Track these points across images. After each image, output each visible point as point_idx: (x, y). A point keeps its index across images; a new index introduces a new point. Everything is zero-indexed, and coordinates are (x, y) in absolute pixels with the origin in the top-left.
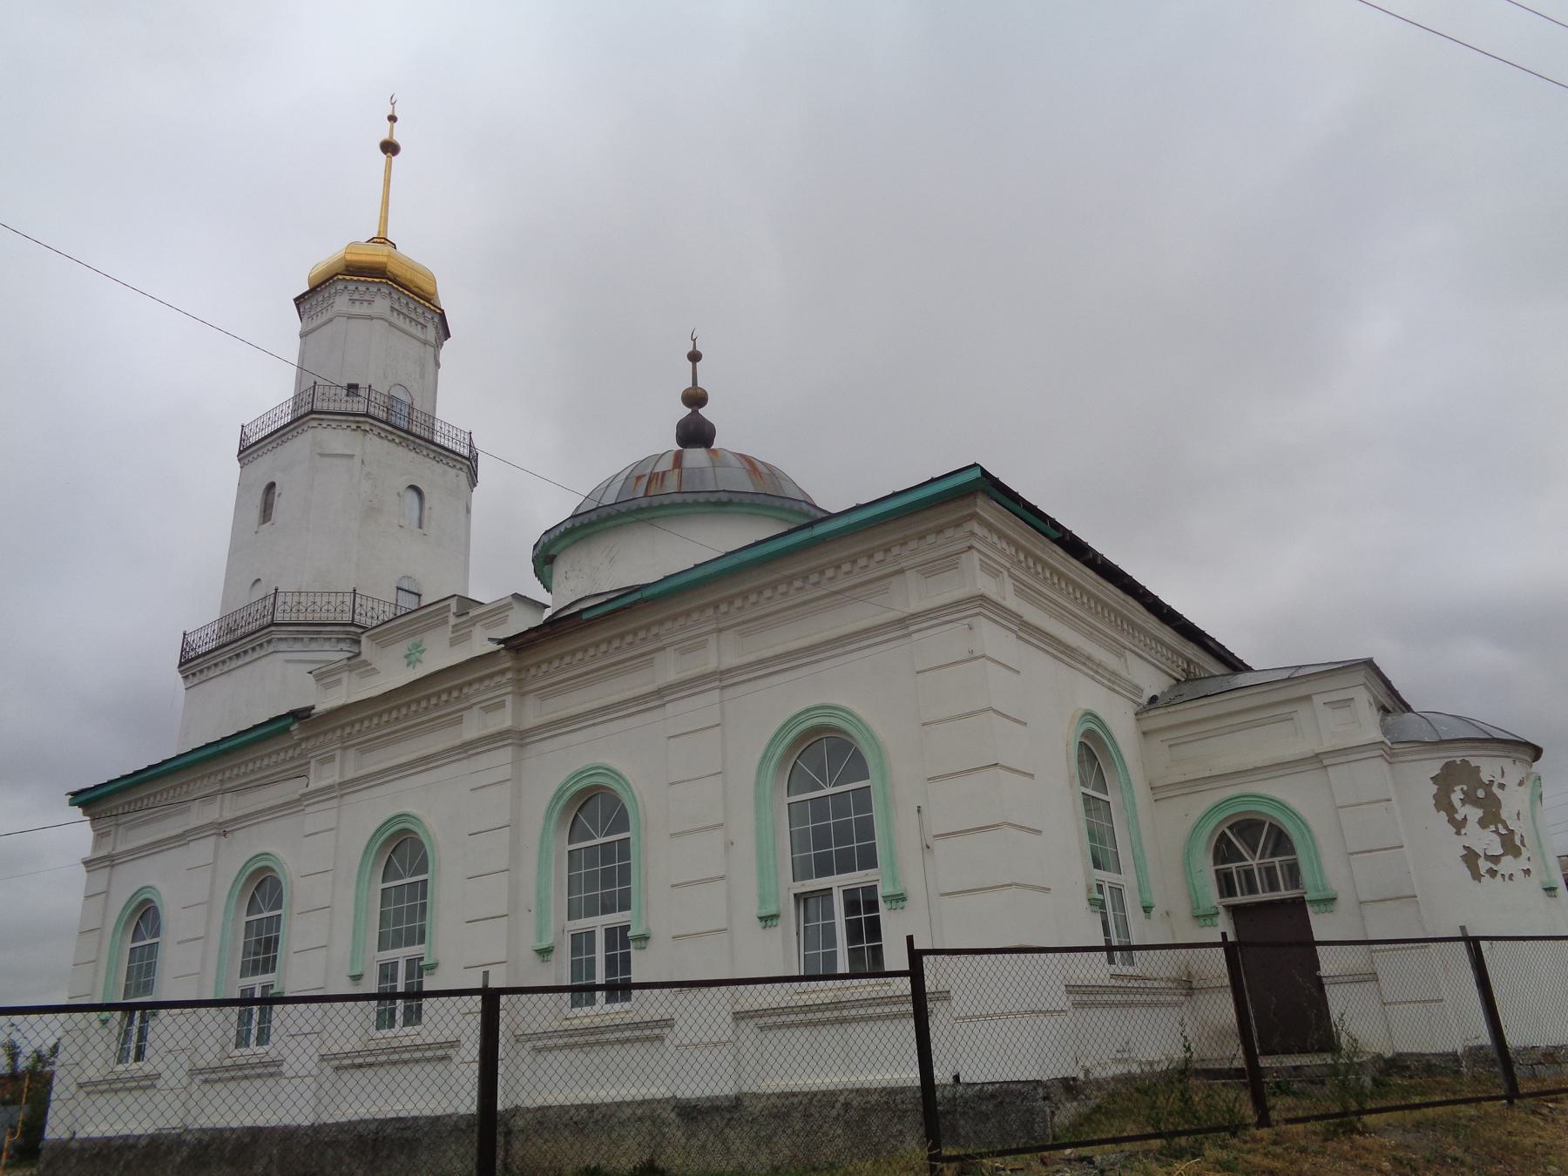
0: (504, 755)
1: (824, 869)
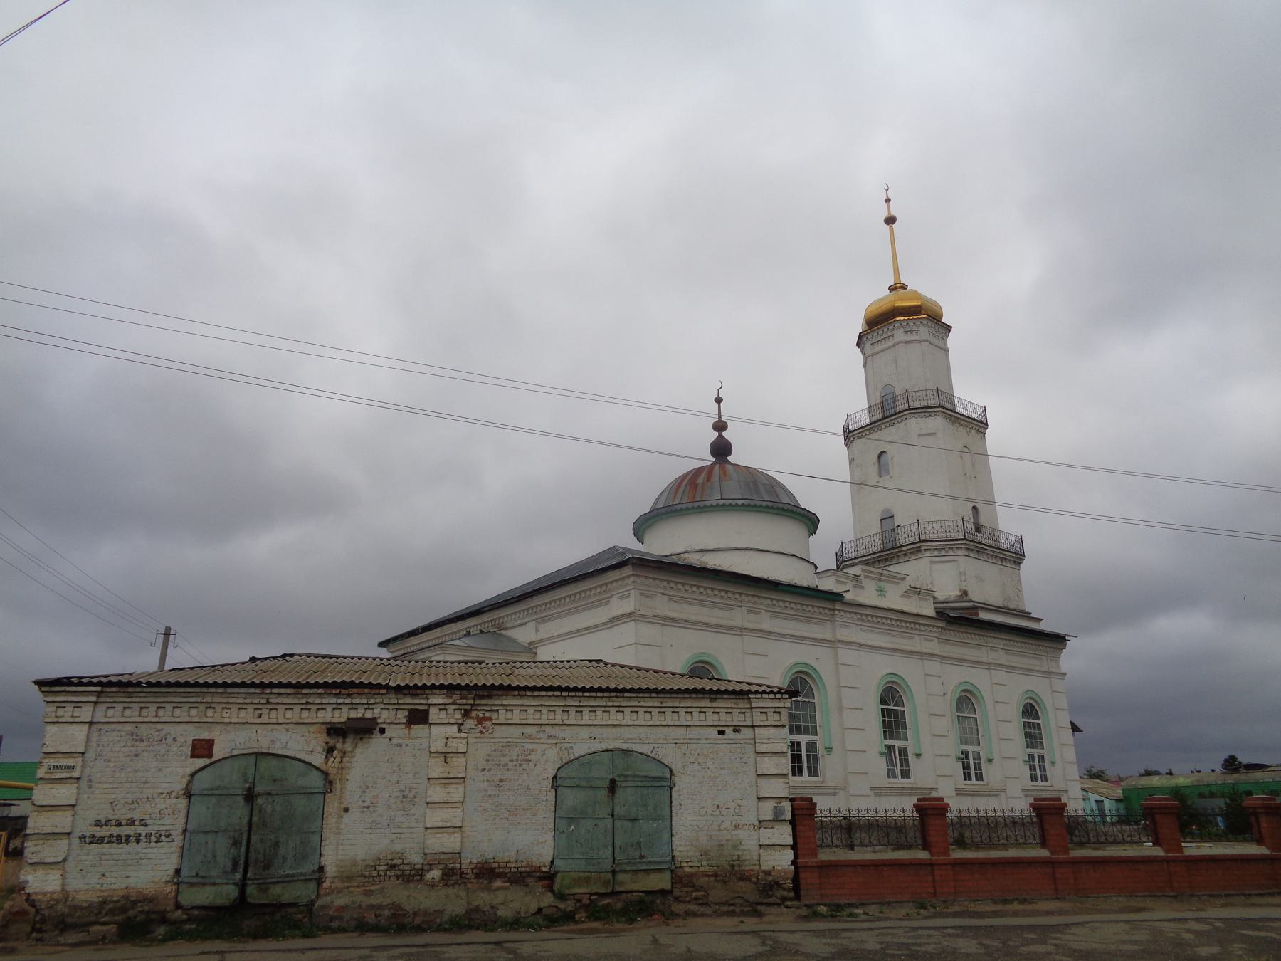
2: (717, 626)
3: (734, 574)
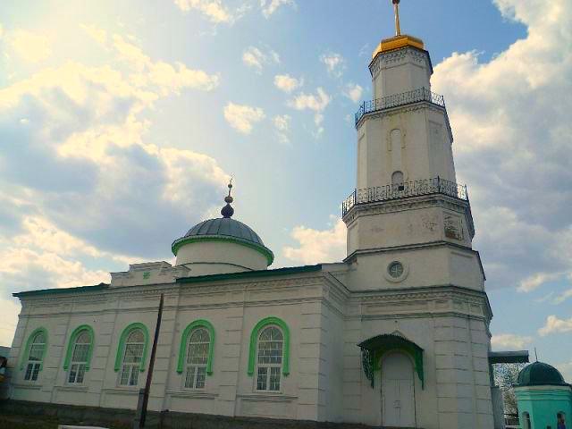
0: (174, 313)
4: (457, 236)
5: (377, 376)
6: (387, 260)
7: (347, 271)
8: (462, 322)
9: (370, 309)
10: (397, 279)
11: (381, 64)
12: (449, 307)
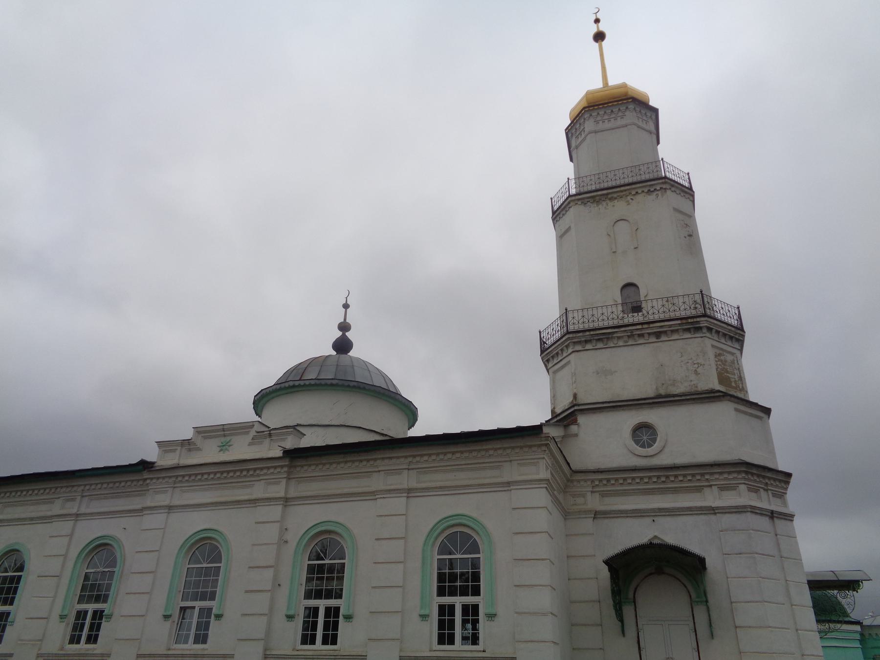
1: (452, 593)
2: (32, 519)
3: (130, 465)
4: (733, 384)
5: (628, 611)
6: (631, 419)
7: (563, 437)
8: (764, 522)
9: (607, 500)
10: (650, 451)
11: (589, 125)
12: (742, 497)
